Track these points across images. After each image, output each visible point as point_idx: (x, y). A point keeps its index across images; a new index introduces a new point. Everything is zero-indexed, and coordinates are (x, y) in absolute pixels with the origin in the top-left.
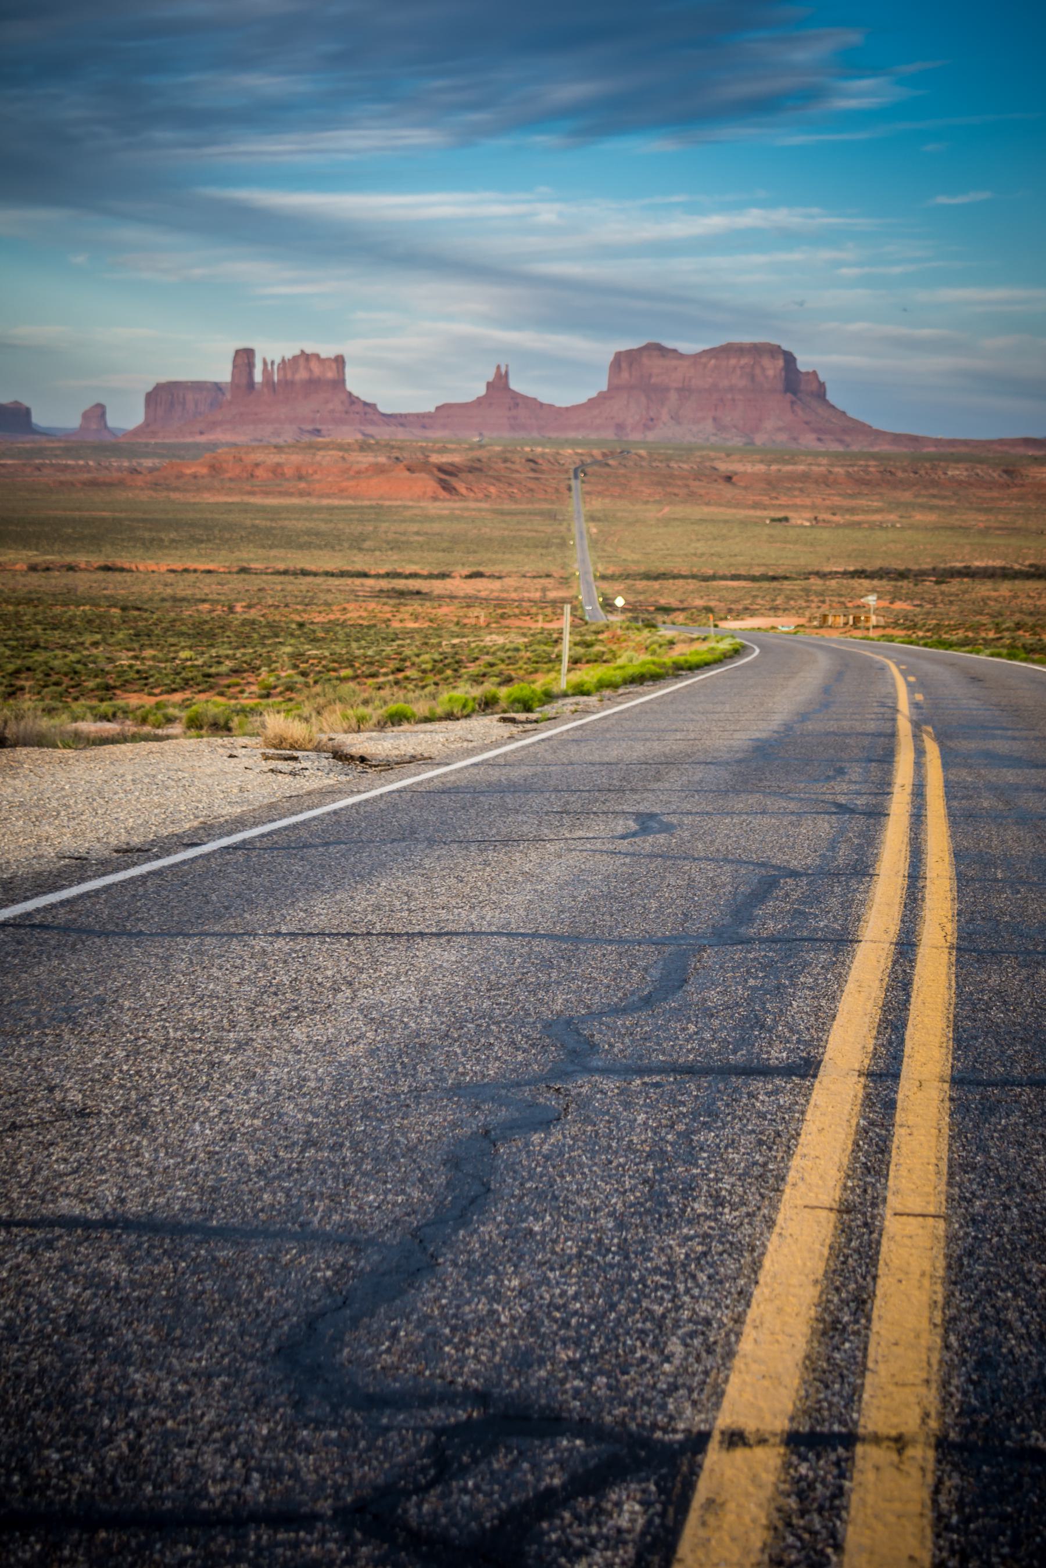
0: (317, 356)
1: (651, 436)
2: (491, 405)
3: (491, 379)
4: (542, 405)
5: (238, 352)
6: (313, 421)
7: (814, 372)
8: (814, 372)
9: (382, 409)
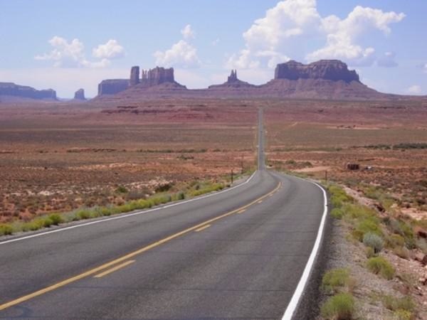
0: (162, 69)
1: (291, 96)
6: (162, 93)
9: (188, 88)
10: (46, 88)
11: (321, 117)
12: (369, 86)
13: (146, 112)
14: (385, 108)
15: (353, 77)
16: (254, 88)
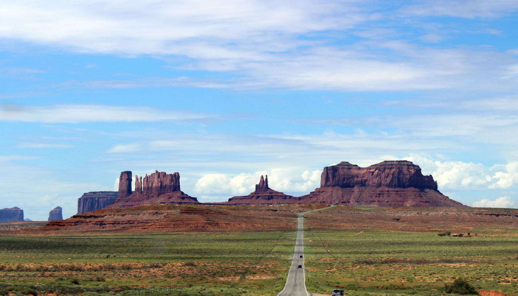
0: (165, 174)
2: (258, 197)
3: (258, 184)
4: (286, 196)
5: (123, 174)
7: (431, 176)
8: (431, 176)
9: (200, 201)
10: (10, 205)
11: (400, 225)
12: (450, 198)
14: (498, 215)
15: (429, 183)
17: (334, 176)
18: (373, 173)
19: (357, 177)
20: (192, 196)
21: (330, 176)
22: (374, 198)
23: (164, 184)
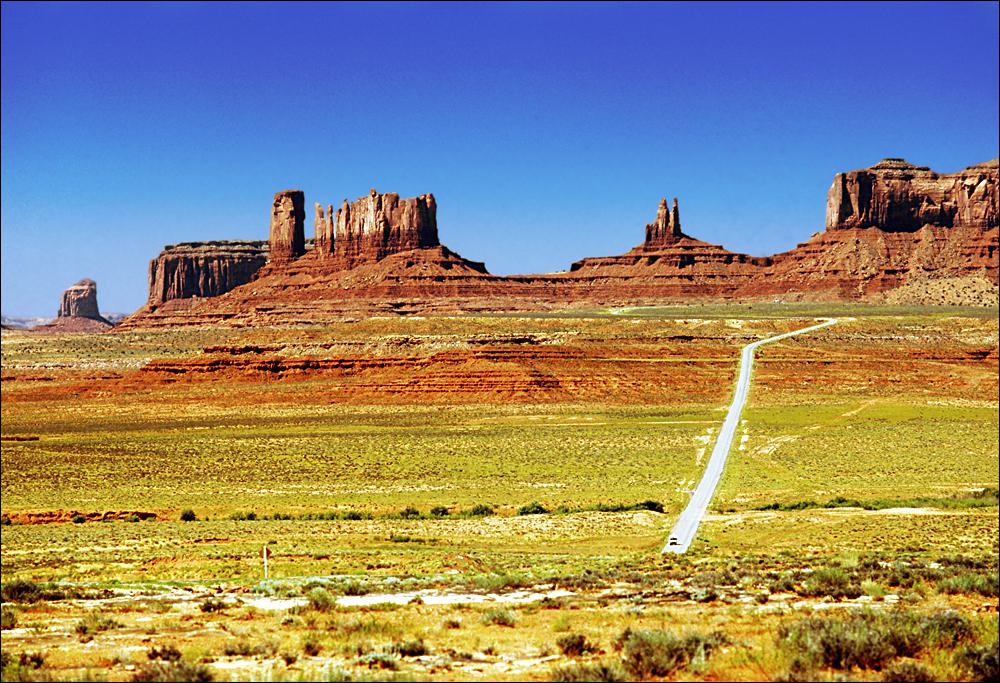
2: (653, 259)
3: (652, 223)
9: (493, 270)
13: (309, 366)
16: (747, 268)
17: (863, 203)
18: (972, 188)
19: (930, 202)
20: (470, 259)
21: (853, 197)
22: (975, 260)
23: (394, 228)
